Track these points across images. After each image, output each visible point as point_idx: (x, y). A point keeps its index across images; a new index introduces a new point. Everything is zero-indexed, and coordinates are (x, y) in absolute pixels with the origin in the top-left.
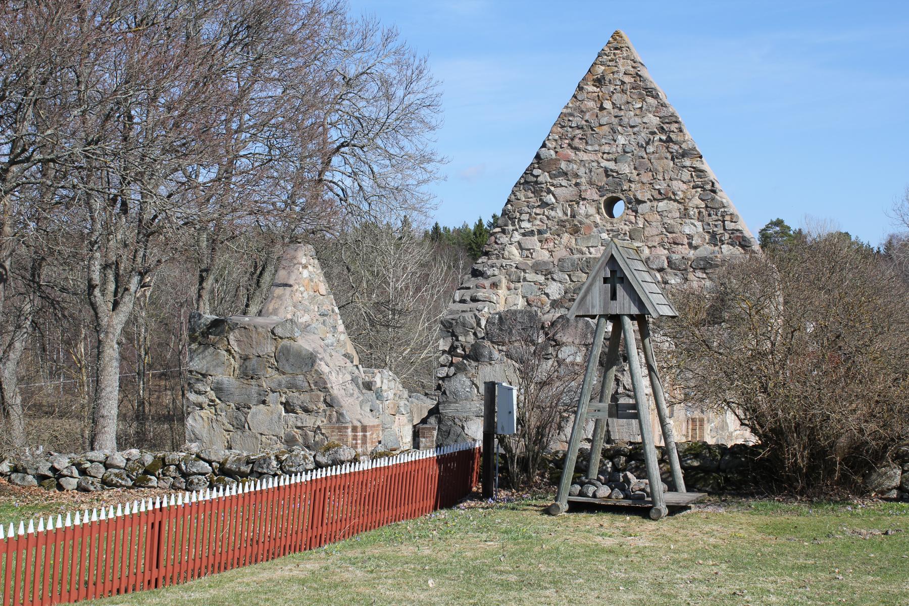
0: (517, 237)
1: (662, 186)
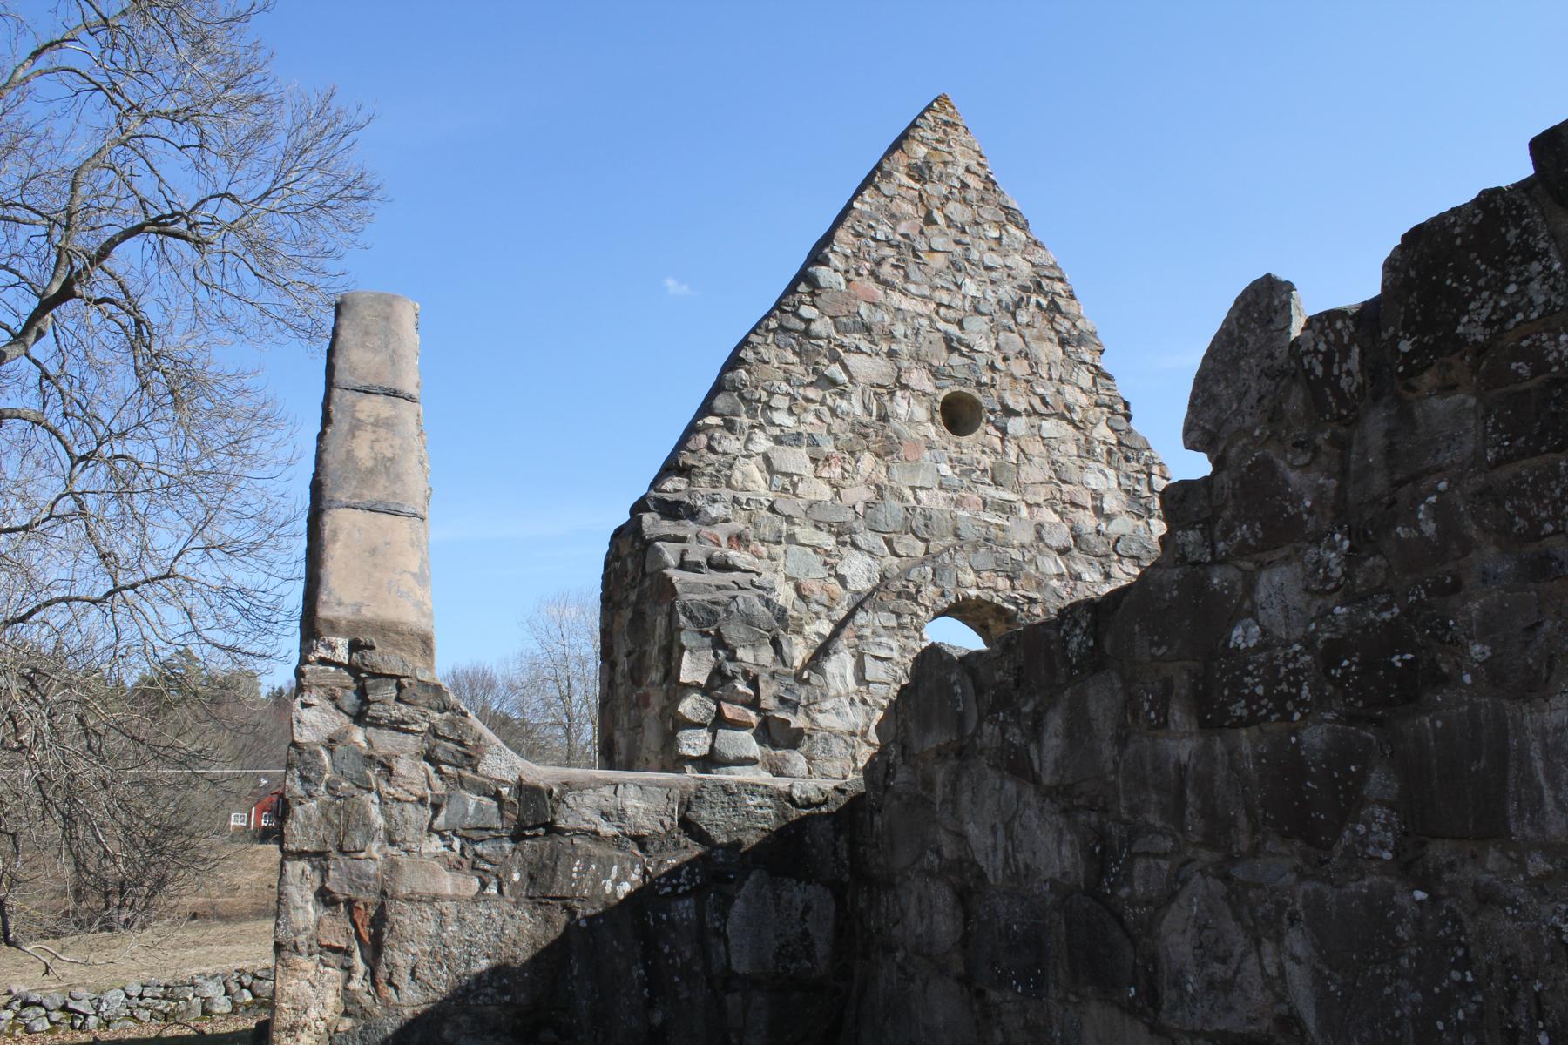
0: (762, 443)
1: (1047, 390)
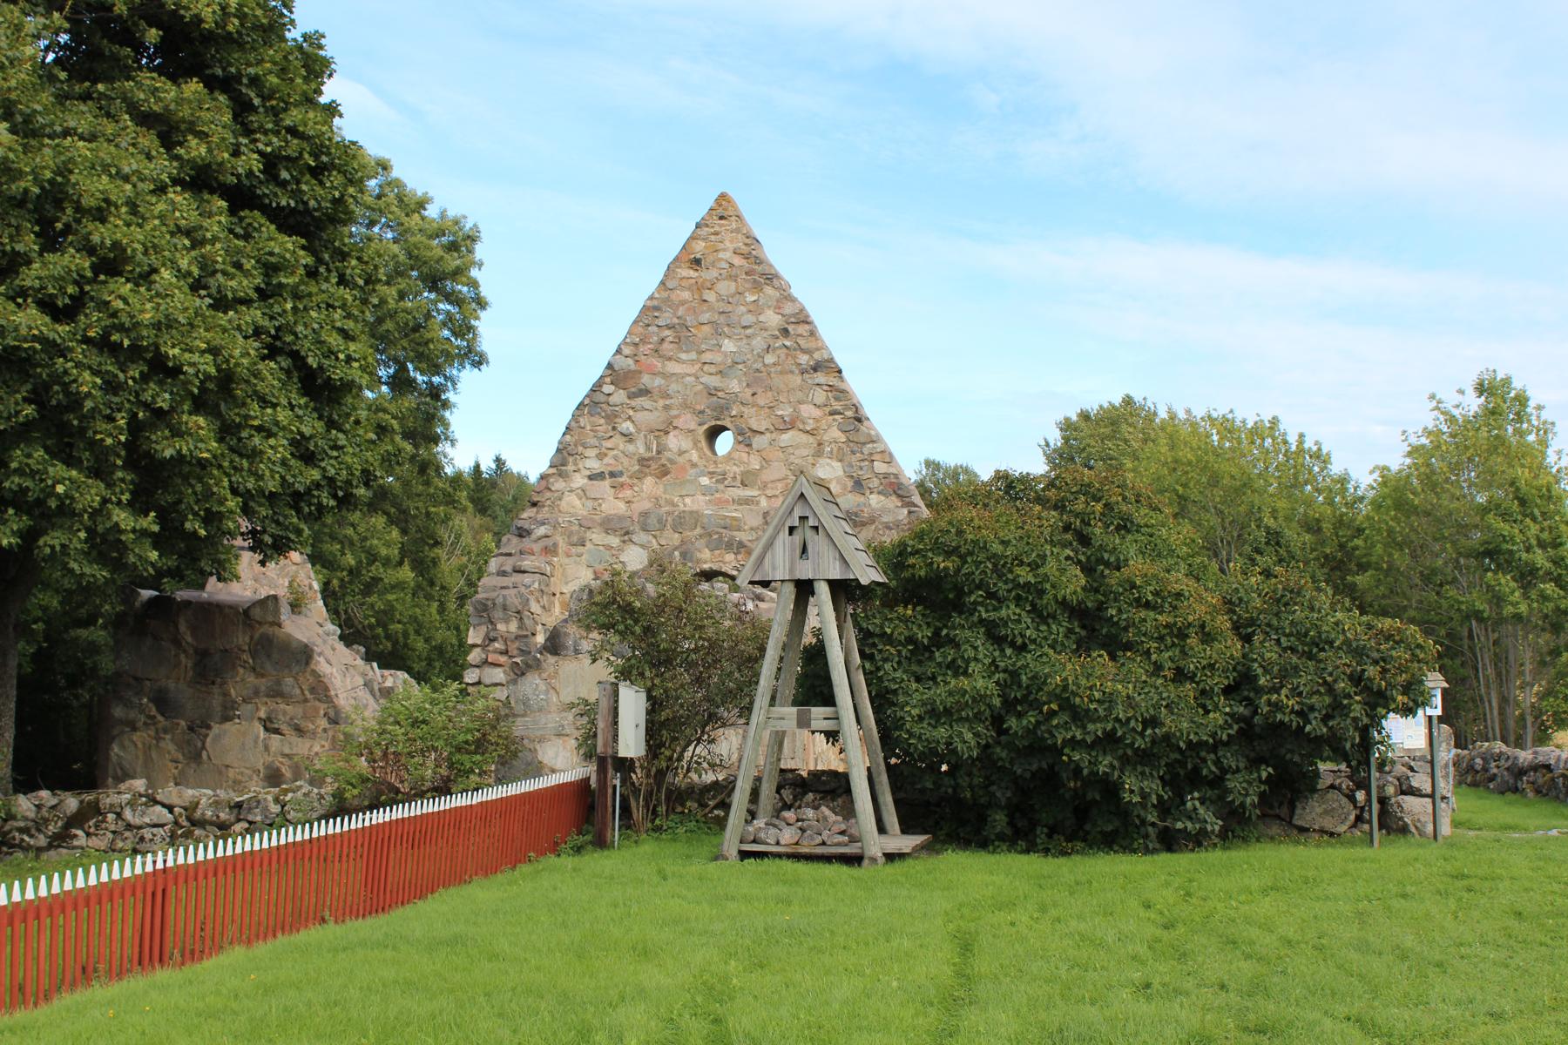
1: (785, 411)
